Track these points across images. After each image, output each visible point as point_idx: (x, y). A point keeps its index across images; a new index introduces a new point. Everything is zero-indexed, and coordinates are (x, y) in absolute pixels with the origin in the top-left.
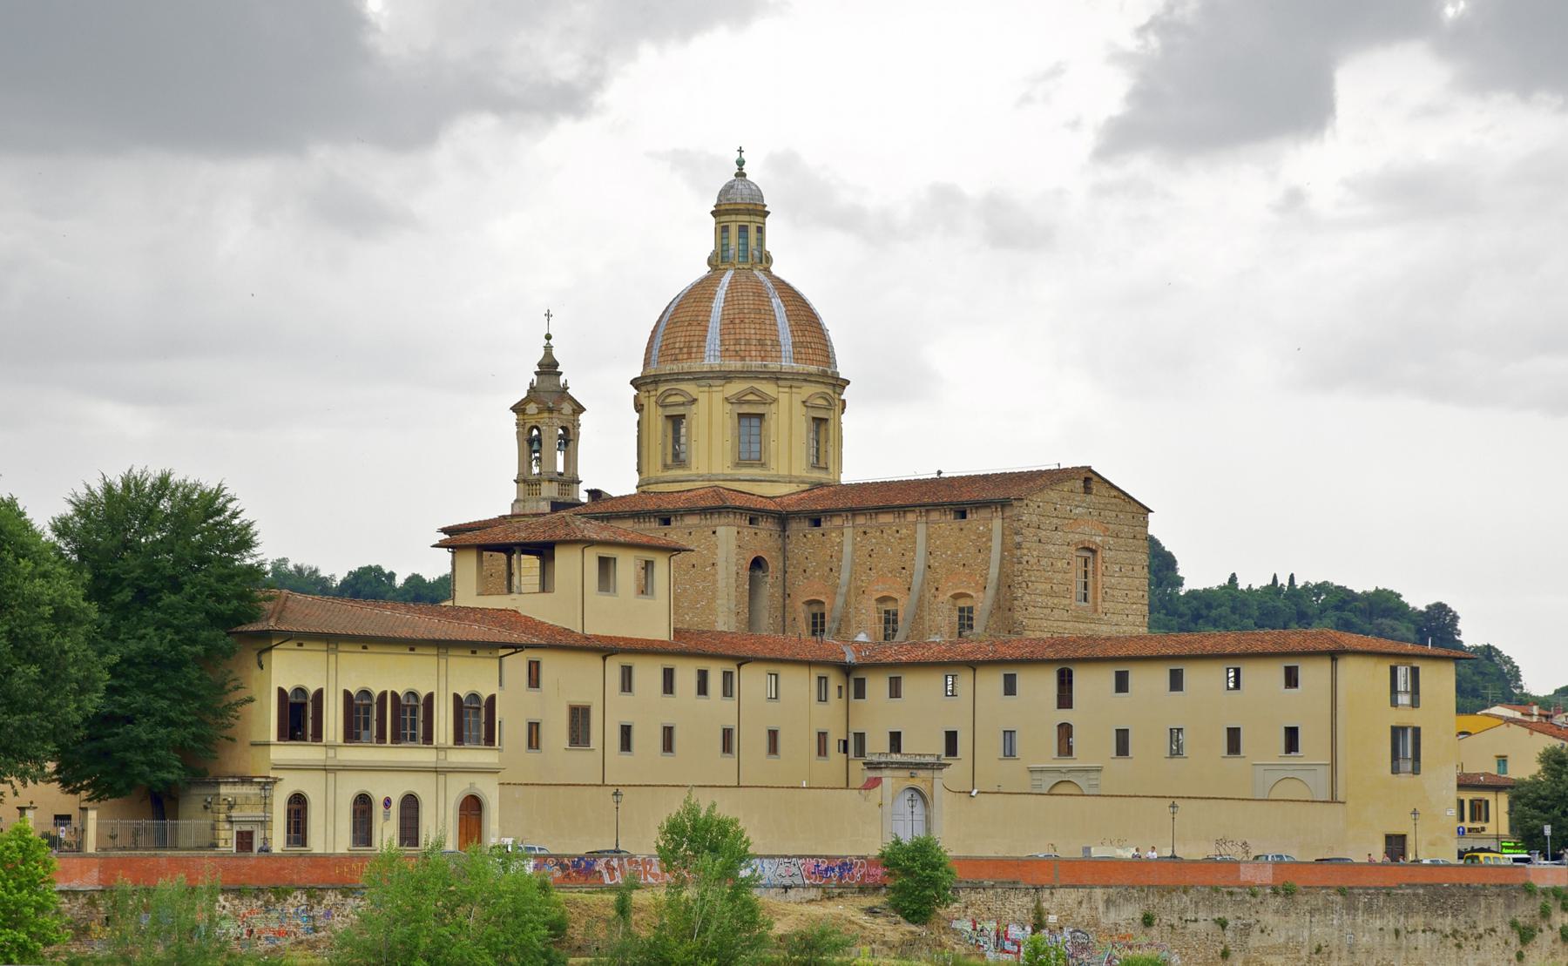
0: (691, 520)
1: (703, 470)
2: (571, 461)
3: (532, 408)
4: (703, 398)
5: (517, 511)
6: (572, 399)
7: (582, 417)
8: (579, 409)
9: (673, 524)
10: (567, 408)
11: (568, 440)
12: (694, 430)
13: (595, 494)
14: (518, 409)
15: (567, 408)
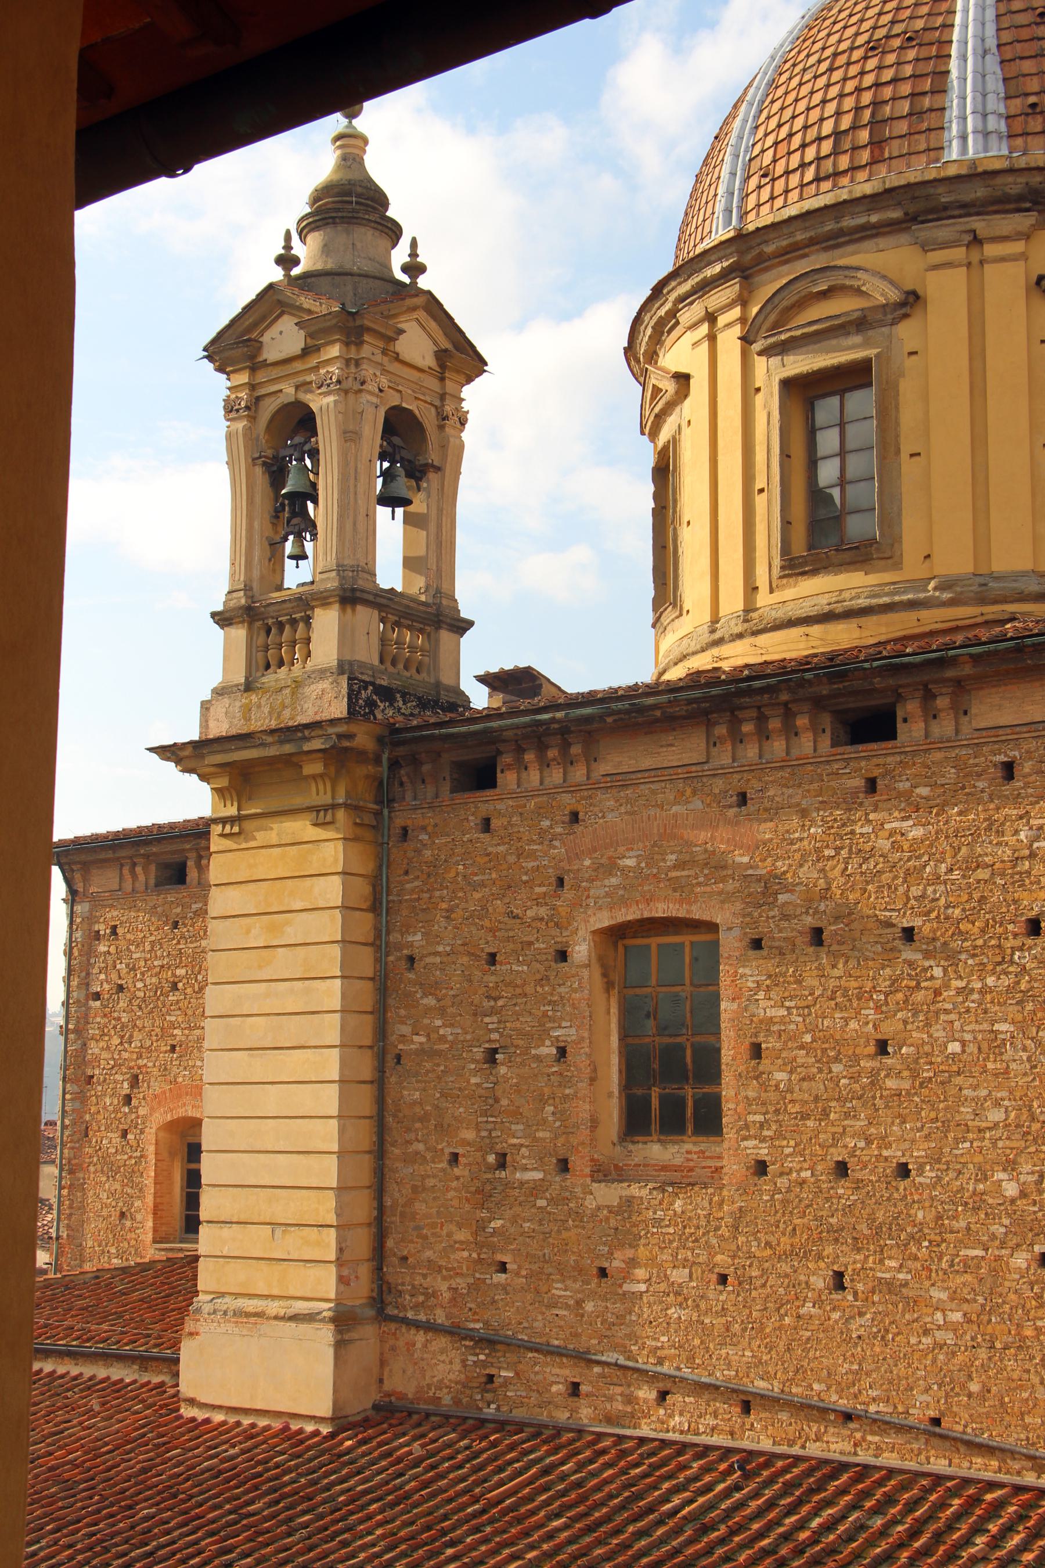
0: (1000, 708)
1: (956, 560)
2: (434, 555)
3: (284, 339)
4: (946, 290)
5: (219, 728)
6: (433, 306)
7: (474, 396)
8: (461, 358)
9: (911, 730)
10: (417, 344)
11: (416, 455)
12: (908, 416)
13: (516, 683)
14: (234, 347)
15: (417, 344)
